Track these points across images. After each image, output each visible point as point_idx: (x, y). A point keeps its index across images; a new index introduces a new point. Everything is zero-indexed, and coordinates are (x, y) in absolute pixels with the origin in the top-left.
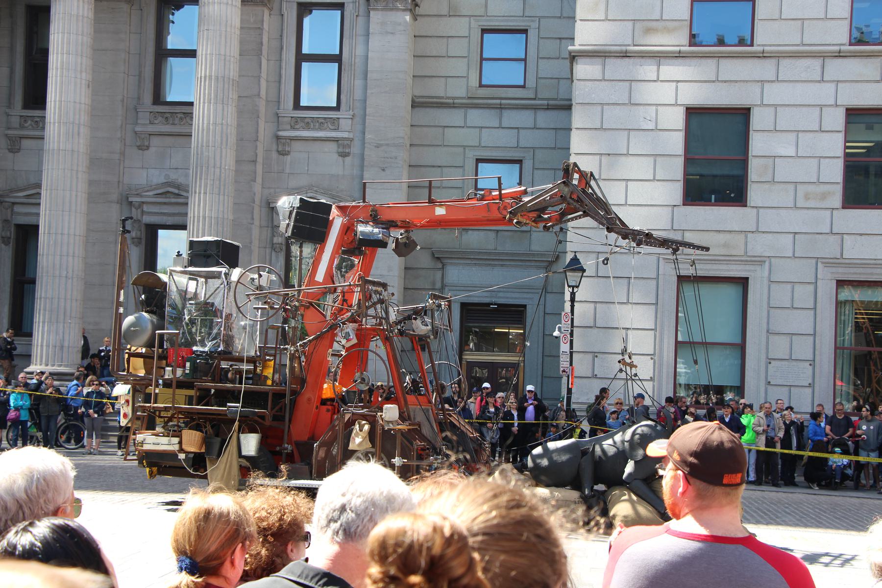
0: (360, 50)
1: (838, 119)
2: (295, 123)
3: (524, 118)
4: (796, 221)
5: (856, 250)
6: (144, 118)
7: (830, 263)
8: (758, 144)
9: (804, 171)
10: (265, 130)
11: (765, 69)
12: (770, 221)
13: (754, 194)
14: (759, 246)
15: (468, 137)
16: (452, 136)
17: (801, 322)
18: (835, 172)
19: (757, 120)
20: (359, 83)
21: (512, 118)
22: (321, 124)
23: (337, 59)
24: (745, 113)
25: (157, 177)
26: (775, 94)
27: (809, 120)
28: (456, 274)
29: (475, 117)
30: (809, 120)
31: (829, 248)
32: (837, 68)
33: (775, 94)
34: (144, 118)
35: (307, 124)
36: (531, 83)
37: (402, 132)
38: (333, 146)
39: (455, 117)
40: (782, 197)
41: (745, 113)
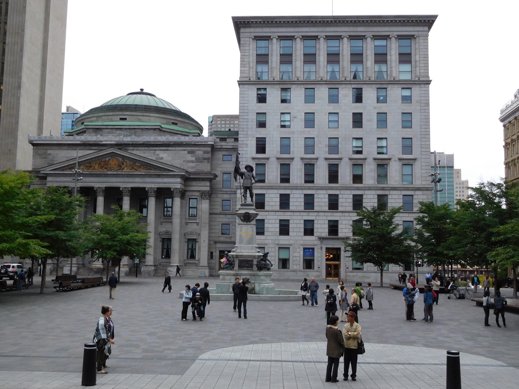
0: (200, 206)
2: (189, 219)
3: (230, 216)
5: (281, 242)
6: (162, 219)
7: (277, 245)
8: (266, 225)
9: (273, 230)
10: (184, 221)
11: (266, 213)
12: (268, 238)
13: (265, 233)
14: (266, 242)
15: (220, 220)
16: (218, 220)
19: (266, 221)
20: (200, 212)
21: (228, 216)
22: (194, 219)
23: (196, 208)
24: (264, 220)
25: (164, 230)
26: (268, 217)
27: (273, 221)
28: (218, 245)
29: (221, 216)
30: (273, 221)
31: (277, 243)
32: (278, 213)
33: (268, 217)
34: (162, 219)
35: (191, 220)
36: (231, 210)
37: (208, 221)
38: (196, 224)
39: (218, 216)
40: (270, 234)
41: (264, 220)
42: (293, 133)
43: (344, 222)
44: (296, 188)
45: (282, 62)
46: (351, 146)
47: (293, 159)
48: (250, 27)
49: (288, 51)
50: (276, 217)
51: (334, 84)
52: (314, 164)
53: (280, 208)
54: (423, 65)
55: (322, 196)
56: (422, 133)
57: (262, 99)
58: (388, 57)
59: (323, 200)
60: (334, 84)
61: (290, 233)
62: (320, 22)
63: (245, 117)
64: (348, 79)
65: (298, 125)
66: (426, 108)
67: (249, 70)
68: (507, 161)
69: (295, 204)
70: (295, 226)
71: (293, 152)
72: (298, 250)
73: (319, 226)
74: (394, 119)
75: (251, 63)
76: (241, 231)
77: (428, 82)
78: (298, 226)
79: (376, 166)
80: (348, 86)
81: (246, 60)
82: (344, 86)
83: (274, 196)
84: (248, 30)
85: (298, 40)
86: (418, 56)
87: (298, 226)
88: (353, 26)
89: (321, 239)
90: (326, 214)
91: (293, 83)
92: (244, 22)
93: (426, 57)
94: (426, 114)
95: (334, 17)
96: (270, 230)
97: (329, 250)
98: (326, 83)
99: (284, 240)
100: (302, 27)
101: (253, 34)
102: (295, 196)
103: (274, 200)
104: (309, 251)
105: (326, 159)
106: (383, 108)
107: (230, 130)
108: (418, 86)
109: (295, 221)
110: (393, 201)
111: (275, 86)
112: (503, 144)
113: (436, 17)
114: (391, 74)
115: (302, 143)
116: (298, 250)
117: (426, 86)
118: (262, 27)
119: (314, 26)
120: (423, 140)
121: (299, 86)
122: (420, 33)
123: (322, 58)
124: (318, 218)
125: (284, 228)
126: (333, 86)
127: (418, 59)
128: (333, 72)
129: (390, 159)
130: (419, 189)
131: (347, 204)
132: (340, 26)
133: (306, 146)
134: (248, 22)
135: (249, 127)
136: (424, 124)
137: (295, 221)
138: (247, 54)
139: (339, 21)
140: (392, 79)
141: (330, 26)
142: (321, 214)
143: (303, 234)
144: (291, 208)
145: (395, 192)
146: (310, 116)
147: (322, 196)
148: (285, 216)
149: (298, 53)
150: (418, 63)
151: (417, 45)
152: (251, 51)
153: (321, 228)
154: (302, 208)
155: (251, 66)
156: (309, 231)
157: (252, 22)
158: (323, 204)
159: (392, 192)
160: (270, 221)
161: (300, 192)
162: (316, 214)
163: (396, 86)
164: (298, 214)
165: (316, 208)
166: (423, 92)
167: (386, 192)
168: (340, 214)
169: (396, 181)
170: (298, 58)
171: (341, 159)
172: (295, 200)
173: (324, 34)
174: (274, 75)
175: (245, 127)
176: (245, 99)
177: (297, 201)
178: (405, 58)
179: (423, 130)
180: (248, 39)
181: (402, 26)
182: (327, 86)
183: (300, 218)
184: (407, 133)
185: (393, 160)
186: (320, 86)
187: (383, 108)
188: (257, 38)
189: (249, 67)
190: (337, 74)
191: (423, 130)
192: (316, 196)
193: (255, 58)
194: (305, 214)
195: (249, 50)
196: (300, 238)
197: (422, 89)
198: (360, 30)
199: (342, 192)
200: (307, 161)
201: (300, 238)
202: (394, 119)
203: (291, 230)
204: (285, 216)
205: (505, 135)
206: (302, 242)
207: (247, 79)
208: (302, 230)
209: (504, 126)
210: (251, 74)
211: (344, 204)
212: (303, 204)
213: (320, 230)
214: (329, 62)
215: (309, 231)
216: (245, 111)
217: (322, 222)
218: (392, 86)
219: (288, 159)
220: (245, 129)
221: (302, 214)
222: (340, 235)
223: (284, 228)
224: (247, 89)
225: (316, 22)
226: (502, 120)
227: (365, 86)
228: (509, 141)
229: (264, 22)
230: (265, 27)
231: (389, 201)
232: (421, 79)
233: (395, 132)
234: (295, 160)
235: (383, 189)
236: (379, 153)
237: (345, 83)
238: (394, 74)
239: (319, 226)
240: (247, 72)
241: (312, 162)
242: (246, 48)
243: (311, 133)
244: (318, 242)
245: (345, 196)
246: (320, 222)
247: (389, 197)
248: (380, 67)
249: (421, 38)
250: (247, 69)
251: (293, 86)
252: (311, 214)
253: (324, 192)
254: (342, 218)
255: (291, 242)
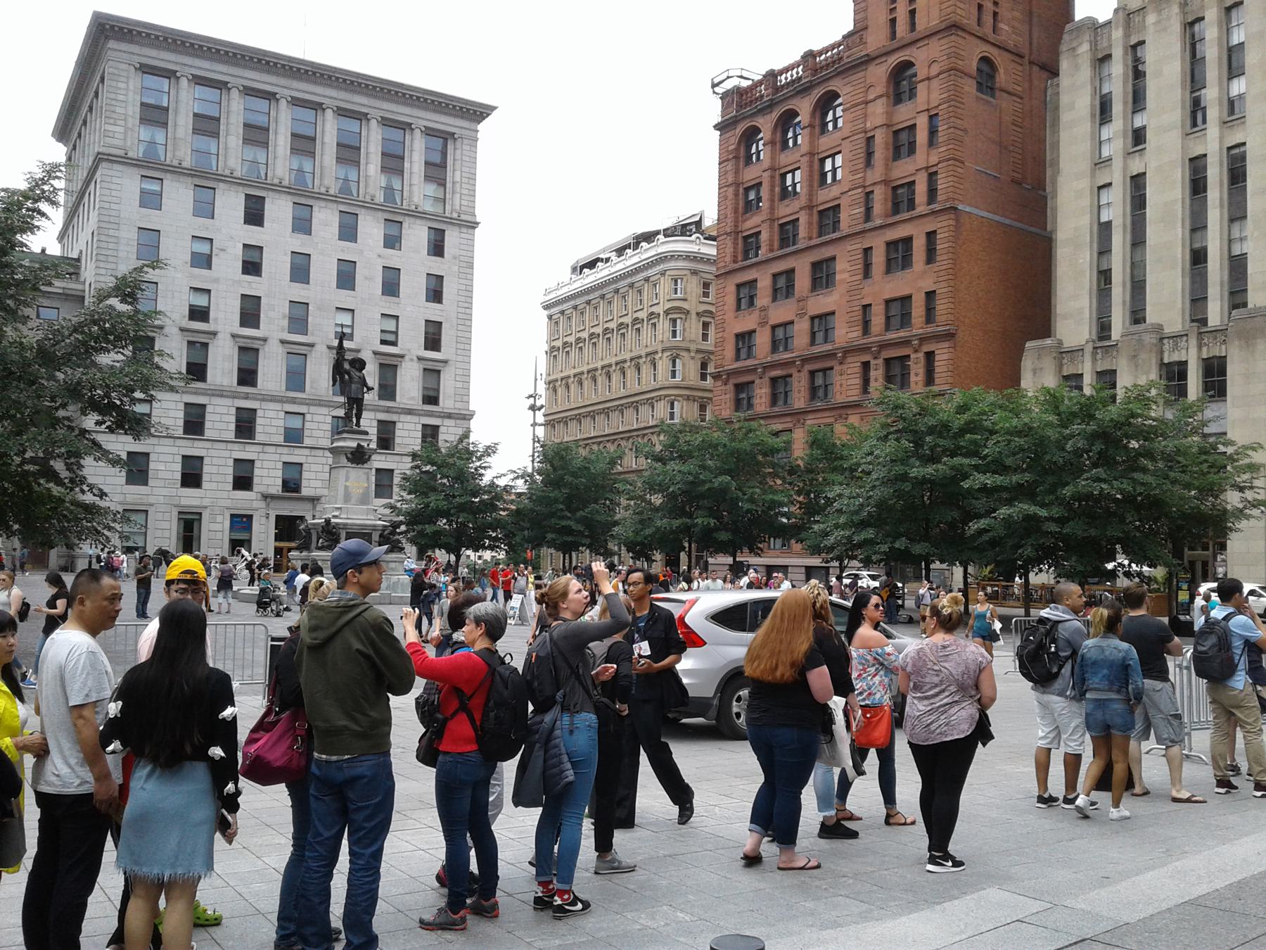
1: (179, 459)
4: (165, 492)
5: (184, 502)
8: (152, 466)
9: (168, 475)
12: (156, 491)
13: (151, 482)
14: (152, 500)
17: (166, 525)
18: (179, 476)
19: (152, 457)
26: (158, 449)
27: (170, 458)
30: (170, 458)
40: (161, 483)
42: (216, 280)
43: (314, 467)
44: (220, 393)
45: (196, 131)
46: (332, 323)
47: (214, 334)
48: (131, 42)
49: (212, 111)
50: (175, 450)
51: (305, 200)
52: (257, 350)
53: (185, 433)
54: (466, 192)
55: (272, 414)
56: (460, 316)
57: (151, 200)
58: (406, 165)
59: (274, 422)
60: (305, 200)
61: (205, 485)
62: (284, 66)
63: (111, 232)
64: (332, 192)
65: (228, 263)
66: (468, 271)
67: (125, 133)
68: (552, 378)
69: (217, 425)
70: (214, 469)
71: (216, 319)
72: (219, 519)
73: (265, 472)
74: (413, 286)
75: (130, 120)
76: (347, 479)
77: (473, 225)
78: (222, 470)
79: (377, 366)
80: (330, 204)
81: (118, 110)
82: (323, 204)
83: (172, 405)
84: (124, 46)
85: (235, 93)
86: (458, 174)
87: (222, 470)
88: (346, 90)
89: (266, 497)
90: (280, 450)
91: (221, 178)
92: (121, 29)
93: (472, 177)
94: (468, 282)
95: (312, 64)
96: (161, 475)
97: (279, 519)
98: (289, 191)
99: (191, 498)
100: (245, 67)
101: (137, 60)
102: (218, 409)
103: (172, 414)
104: (241, 522)
105: (283, 342)
106: (394, 258)
107: (43, 250)
108: (457, 228)
109: (215, 461)
110: (405, 433)
111: (182, 178)
112: (546, 347)
113: (495, 108)
114: (410, 197)
115: (235, 306)
116: (219, 519)
117: (470, 231)
118: (158, 48)
119: (268, 72)
120: (460, 327)
121: (234, 188)
122: (464, 132)
123: (281, 140)
124: (262, 456)
125: (192, 476)
126: (303, 201)
127: (458, 178)
128: (300, 171)
129: (402, 356)
130: (450, 416)
131: (321, 434)
132: (320, 84)
133: (292, 319)
134: (130, 31)
135: (120, 254)
136: (463, 299)
137: (215, 461)
138: (121, 97)
139: (322, 75)
140: (413, 208)
141: (301, 79)
142: (268, 449)
143: (230, 487)
144: (208, 433)
145: (409, 418)
146: (256, 254)
147: (272, 414)
148: (194, 448)
149: (233, 119)
150: (458, 186)
151: (458, 152)
152: (131, 94)
153: (268, 477)
154: (231, 435)
155: (130, 125)
156: (243, 481)
157: (140, 33)
158: (273, 430)
159: (403, 418)
160: (162, 458)
161: (228, 402)
162: (259, 448)
163: (418, 221)
164: (223, 445)
165: (259, 437)
166: (465, 242)
167: (393, 417)
168: (307, 452)
169: (413, 398)
170: (232, 128)
171: (312, 345)
172: (217, 418)
173: (287, 92)
174: (180, 154)
175: (109, 253)
176: (114, 193)
177: (221, 419)
178: (436, 171)
179: (460, 310)
180: (125, 66)
181: (435, 111)
182: (289, 197)
183: (227, 454)
184: (434, 312)
185: (407, 358)
186: (277, 196)
187: (394, 258)
188: (146, 69)
189: (126, 129)
190: (309, 177)
191: (460, 310)
192: (259, 413)
193: (138, 110)
194: (236, 447)
195: (127, 89)
196: (225, 495)
197: (463, 235)
198: (359, 102)
199: (313, 409)
200: (243, 343)
201: (225, 495)
202: (413, 286)
203: (205, 477)
204: (194, 448)
205: (551, 334)
206: (228, 503)
207: (121, 153)
208: (230, 479)
209: (550, 317)
210: (129, 143)
211: (315, 433)
212: (233, 427)
213: (266, 481)
214: (295, 150)
215: (243, 481)
216: (112, 219)
217: (271, 465)
218: (412, 220)
219: (204, 332)
220: (110, 259)
221: (230, 446)
222: (305, 492)
223: (192, 476)
224: (119, 174)
225: (276, 64)
226: (546, 307)
227: (363, 210)
228: (559, 344)
229: (166, 39)
230: (164, 49)
231: (398, 433)
232: (463, 217)
233: (413, 309)
234: (220, 336)
235: (388, 410)
236: (383, 342)
237: (325, 197)
238: (416, 200)
239: (265, 472)
240: (121, 136)
241: (256, 345)
242: (120, 85)
243: (252, 285)
244: (262, 504)
245: (316, 418)
246: (266, 464)
247: (399, 426)
248: (389, 181)
249: (465, 141)
250: (122, 129)
251: (222, 185)
252: (248, 448)
253: (278, 406)
254: (310, 459)
255: (206, 502)
